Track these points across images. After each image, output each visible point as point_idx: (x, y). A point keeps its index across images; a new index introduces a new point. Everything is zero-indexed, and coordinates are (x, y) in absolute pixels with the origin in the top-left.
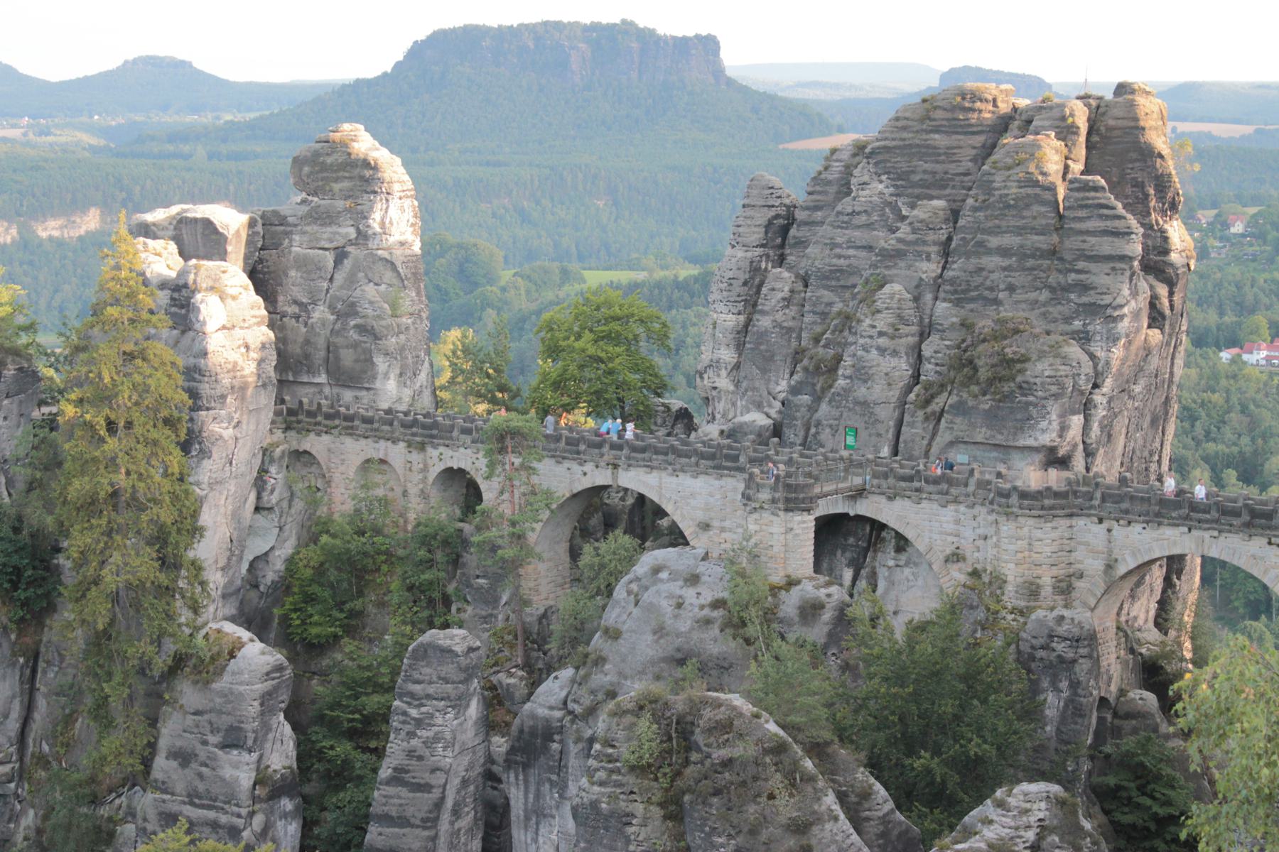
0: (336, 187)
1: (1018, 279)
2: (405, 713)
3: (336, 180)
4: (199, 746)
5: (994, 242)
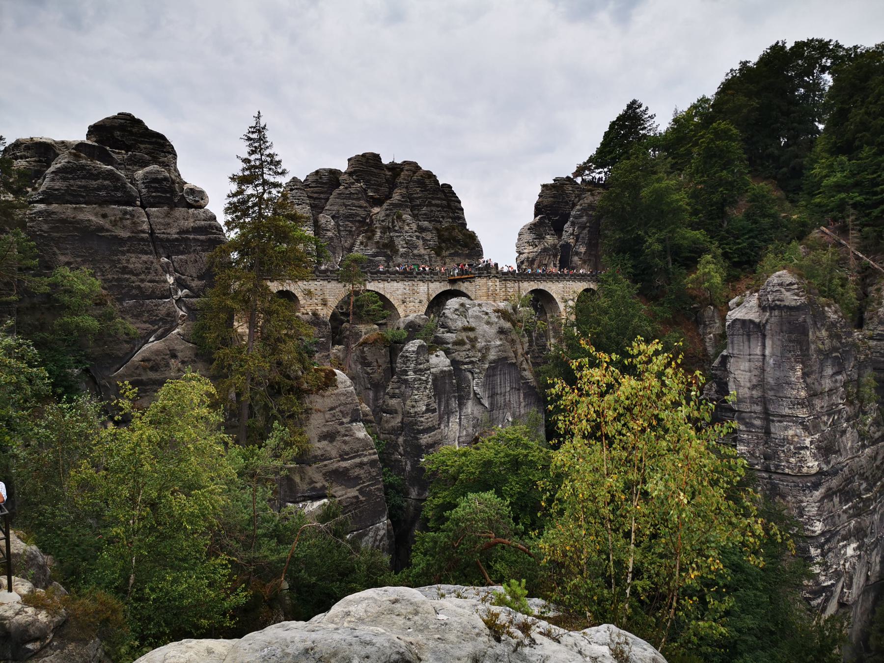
0: (142, 146)
1: (445, 215)
2: (420, 379)
5: (433, 202)
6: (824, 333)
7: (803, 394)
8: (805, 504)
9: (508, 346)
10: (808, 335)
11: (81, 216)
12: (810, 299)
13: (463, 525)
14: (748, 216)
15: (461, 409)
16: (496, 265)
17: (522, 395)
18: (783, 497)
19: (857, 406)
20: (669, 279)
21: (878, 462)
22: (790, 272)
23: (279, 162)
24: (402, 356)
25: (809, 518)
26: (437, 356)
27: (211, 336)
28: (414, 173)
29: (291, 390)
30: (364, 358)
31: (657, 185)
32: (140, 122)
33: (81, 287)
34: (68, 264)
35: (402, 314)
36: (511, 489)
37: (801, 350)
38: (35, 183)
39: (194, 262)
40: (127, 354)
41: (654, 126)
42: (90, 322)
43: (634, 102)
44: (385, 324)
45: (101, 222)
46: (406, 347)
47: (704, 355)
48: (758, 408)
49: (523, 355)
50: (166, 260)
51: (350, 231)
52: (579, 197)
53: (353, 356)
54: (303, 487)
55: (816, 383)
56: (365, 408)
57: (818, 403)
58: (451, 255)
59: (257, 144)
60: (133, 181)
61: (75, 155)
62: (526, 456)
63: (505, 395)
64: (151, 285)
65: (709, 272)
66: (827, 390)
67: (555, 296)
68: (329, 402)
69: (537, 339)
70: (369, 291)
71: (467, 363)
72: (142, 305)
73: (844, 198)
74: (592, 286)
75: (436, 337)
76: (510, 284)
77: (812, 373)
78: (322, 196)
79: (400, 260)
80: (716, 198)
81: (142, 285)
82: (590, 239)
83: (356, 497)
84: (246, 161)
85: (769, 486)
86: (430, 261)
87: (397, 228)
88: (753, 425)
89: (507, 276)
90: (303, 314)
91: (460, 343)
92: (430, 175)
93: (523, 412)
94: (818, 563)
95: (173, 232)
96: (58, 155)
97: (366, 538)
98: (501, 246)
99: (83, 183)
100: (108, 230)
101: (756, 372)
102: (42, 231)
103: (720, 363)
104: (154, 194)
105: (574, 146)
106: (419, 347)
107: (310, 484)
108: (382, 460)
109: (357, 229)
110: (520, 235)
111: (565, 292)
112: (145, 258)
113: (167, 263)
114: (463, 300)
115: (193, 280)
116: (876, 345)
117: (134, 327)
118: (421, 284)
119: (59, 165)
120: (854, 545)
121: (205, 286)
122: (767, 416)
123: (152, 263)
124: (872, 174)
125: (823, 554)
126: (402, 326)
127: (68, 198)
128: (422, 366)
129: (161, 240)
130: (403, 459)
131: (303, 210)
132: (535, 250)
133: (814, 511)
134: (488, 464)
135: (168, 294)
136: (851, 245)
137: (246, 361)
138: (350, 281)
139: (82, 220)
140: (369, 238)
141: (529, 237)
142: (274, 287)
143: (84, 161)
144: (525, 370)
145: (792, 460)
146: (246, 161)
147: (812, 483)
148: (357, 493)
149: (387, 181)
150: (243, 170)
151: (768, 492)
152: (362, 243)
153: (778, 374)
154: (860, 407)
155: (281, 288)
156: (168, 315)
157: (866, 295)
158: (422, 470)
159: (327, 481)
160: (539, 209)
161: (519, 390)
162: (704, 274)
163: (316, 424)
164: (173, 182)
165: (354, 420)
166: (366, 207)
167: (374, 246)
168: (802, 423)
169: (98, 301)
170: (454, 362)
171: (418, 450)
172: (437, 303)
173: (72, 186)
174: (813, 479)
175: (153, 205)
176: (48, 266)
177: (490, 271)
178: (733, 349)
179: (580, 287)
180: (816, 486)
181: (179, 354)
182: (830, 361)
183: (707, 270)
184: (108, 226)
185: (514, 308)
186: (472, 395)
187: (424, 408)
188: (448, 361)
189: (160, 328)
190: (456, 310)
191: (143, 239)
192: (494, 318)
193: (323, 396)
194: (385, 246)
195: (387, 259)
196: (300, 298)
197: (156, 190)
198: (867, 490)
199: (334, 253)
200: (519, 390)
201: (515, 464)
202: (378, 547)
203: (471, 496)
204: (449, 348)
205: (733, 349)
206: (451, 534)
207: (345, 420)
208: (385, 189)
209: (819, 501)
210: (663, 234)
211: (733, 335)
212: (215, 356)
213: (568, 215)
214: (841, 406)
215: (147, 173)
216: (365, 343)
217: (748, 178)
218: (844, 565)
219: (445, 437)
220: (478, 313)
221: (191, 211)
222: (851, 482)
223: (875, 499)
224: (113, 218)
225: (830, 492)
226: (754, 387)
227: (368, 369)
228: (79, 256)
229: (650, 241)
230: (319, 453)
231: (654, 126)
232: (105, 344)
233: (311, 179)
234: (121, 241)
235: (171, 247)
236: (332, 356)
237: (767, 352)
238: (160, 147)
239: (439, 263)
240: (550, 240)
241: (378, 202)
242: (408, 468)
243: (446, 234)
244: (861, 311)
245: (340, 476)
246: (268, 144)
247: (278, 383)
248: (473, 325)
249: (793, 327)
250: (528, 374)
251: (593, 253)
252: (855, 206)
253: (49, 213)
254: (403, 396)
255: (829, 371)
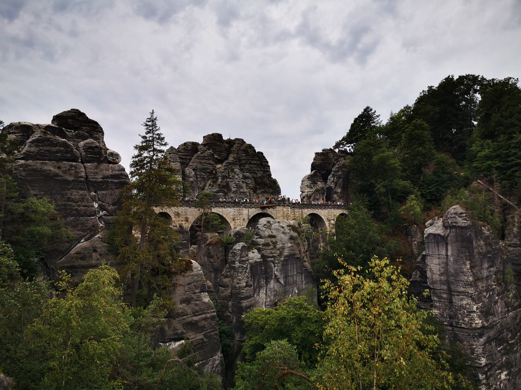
0: (84, 128)
1: (259, 169)
2: (243, 267)
3: (84, 126)
4: (193, 295)
5: (252, 162)
6: (482, 242)
7: (471, 279)
8: (475, 346)
9: (295, 247)
10: (472, 244)
11: (45, 168)
12: (473, 223)
13: (268, 361)
14: (435, 173)
15: (267, 285)
16: (289, 199)
17: (303, 277)
18: (461, 342)
19: (504, 286)
20: (390, 209)
21: (518, 321)
22: (461, 206)
23: (163, 138)
24: (232, 252)
25: (477, 355)
26: (253, 252)
27: (118, 240)
28: (242, 145)
29: (165, 272)
30: (209, 253)
31: (382, 154)
32: (83, 114)
33: (43, 209)
34: (36, 195)
35: (232, 227)
36: (297, 335)
37: (469, 252)
38: (20, 148)
39: (110, 195)
40: (67, 249)
41: (380, 121)
42: (46, 230)
43: (368, 108)
44: (222, 233)
45: (57, 171)
46: (235, 247)
47: (411, 254)
48: (445, 287)
49: (304, 253)
50: (94, 193)
51: (203, 178)
52: (337, 160)
53: (203, 252)
54: (169, 332)
55: (479, 273)
56: (209, 283)
57: (480, 285)
58: (262, 192)
59: (151, 128)
60: (77, 148)
61: (44, 133)
62: (306, 314)
63: (293, 277)
64: (84, 208)
65: (413, 205)
66: (485, 276)
67: (323, 217)
68: (187, 280)
69: (312, 243)
70: (213, 213)
71: (271, 257)
72: (78, 220)
73: (490, 164)
74: (345, 212)
75: (253, 241)
76: (296, 210)
77: (475, 266)
78: (188, 157)
79: (232, 195)
80: (416, 162)
81: (79, 209)
82: (343, 185)
83: (202, 339)
84: (144, 137)
85: (453, 335)
86: (250, 195)
87: (231, 177)
88: (442, 298)
89: (295, 205)
90: (174, 226)
91: (267, 245)
92: (250, 147)
93: (304, 287)
94: (484, 384)
95: (99, 178)
96: (34, 132)
97: (207, 366)
98: (291, 188)
99: (48, 148)
100: (60, 176)
101: (443, 265)
102: (21, 176)
103: (422, 259)
104: (89, 155)
105: (334, 132)
106: (242, 247)
107: (174, 331)
108: (218, 316)
109: (207, 176)
110: (302, 181)
111: (329, 215)
112: (81, 192)
113: (94, 195)
114: (269, 219)
115: (109, 206)
116: (513, 250)
117: (72, 233)
118: (244, 209)
119: (34, 138)
120: (505, 373)
121: (116, 209)
122: (450, 292)
123: (86, 195)
124: (506, 150)
125: (487, 378)
126: (232, 234)
127: (38, 157)
128: (244, 259)
129: (92, 182)
130: (231, 315)
131: (176, 165)
132: (311, 190)
133: (480, 351)
134: (283, 319)
135: (94, 214)
136: (496, 190)
137: (139, 254)
138: (202, 207)
139: (46, 170)
140: (215, 182)
141: (308, 183)
142: (157, 210)
143: (49, 136)
144: (305, 262)
145: (466, 319)
146: (144, 137)
147: (479, 333)
148: (202, 337)
149: (226, 149)
150: (142, 142)
151: (452, 339)
152: (210, 185)
153: (456, 266)
154: (505, 287)
155: (161, 211)
156: (93, 226)
157: (506, 220)
158: (243, 322)
159: (184, 329)
160: (314, 167)
161: (302, 273)
162: (411, 206)
163: (179, 293)
164: (101, 149)
165: (203, 291)
166: (213, 164)
167: (217, 187)
168: (471, 297)
169: (52, 218)
170: (263, 256)
171: (241, 310)
172: (253, 221)
173: (41, 150)
174: (479, 331)
175: (88, 162)
176: (24, 197)
177: (285, 202)
178: (429, 251)
179: (338, 212)
180: (481, 336)
181: (98, 250)
182: (486, 259)
183: (412, 204)
184: (61, 173)
185: (299, 224)
186: (273, 277)
187: (245, 284)
188: (260, 255)
189: (88, 234)
190: (265, 225)
191: (81, 182)
192: (287, 230)
193: (184, 276)
194: (224, 187)
195: (225, 194)
196: (172, 217)
197: (91, 153)
198: (512, 338)
199: (193, 191)
200: (302, 273)
201: (299, 320)
202: (214, 372)
203: (273, 342)
204: (260, 248)
205: (429, 251)
206: (260, 367)
207: (197, 291)
208: (224, 154)
209: (483, 345)
210: (386, 183)
211: (428, 242)
212: (120, 251)
213: (331, 171)
214: (494, 287)
215: (86, 143)
216: (210, 244)
217: (434, 151)
218: (500, 385)
219: (257, 302)
220: (277, 227)
221: (111, 165)
222: (502, 333)
223: (517, 344)
224: (64, 169)
225: (490, 339)
226: (441, 274)
227: (212, 260)
228: (42, 191)
229: (378, 186)
230: (180, 311)
231: (380, 121)
232: (54, 243)
233: (181, 148)
234: (68, 182)
235: (97, 186)
236: (190, 252)
237: (449, 253)
238: (94, 129)
239: (255, 197)
240: (320, 185)
241: (220, 162)
242: (234, 321)
243: (259, 180)
244: (503, 229)
245: (193, 326)
246: (157, 128)
247: (157, 268)
248: (275, 234)
249: (464, 239)
250: (307, 264)
251: (346, 192)
252: (497, 168)
253: (27, 166)
254: (232, 277)
255: (486, 265)
